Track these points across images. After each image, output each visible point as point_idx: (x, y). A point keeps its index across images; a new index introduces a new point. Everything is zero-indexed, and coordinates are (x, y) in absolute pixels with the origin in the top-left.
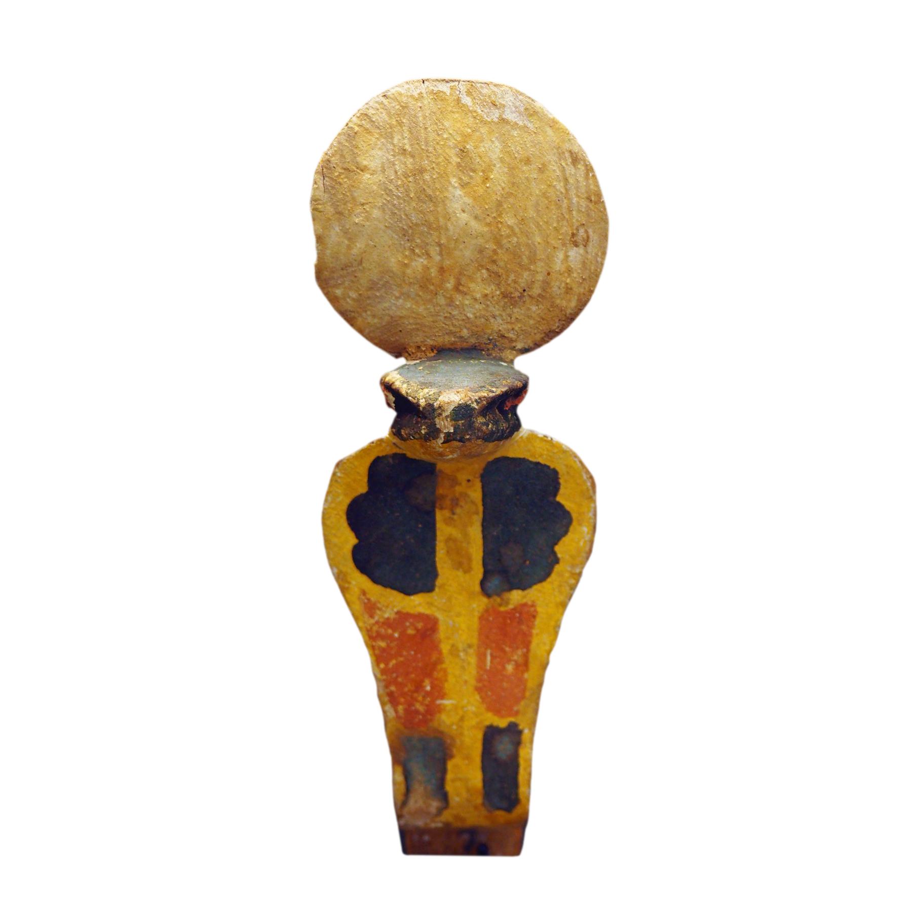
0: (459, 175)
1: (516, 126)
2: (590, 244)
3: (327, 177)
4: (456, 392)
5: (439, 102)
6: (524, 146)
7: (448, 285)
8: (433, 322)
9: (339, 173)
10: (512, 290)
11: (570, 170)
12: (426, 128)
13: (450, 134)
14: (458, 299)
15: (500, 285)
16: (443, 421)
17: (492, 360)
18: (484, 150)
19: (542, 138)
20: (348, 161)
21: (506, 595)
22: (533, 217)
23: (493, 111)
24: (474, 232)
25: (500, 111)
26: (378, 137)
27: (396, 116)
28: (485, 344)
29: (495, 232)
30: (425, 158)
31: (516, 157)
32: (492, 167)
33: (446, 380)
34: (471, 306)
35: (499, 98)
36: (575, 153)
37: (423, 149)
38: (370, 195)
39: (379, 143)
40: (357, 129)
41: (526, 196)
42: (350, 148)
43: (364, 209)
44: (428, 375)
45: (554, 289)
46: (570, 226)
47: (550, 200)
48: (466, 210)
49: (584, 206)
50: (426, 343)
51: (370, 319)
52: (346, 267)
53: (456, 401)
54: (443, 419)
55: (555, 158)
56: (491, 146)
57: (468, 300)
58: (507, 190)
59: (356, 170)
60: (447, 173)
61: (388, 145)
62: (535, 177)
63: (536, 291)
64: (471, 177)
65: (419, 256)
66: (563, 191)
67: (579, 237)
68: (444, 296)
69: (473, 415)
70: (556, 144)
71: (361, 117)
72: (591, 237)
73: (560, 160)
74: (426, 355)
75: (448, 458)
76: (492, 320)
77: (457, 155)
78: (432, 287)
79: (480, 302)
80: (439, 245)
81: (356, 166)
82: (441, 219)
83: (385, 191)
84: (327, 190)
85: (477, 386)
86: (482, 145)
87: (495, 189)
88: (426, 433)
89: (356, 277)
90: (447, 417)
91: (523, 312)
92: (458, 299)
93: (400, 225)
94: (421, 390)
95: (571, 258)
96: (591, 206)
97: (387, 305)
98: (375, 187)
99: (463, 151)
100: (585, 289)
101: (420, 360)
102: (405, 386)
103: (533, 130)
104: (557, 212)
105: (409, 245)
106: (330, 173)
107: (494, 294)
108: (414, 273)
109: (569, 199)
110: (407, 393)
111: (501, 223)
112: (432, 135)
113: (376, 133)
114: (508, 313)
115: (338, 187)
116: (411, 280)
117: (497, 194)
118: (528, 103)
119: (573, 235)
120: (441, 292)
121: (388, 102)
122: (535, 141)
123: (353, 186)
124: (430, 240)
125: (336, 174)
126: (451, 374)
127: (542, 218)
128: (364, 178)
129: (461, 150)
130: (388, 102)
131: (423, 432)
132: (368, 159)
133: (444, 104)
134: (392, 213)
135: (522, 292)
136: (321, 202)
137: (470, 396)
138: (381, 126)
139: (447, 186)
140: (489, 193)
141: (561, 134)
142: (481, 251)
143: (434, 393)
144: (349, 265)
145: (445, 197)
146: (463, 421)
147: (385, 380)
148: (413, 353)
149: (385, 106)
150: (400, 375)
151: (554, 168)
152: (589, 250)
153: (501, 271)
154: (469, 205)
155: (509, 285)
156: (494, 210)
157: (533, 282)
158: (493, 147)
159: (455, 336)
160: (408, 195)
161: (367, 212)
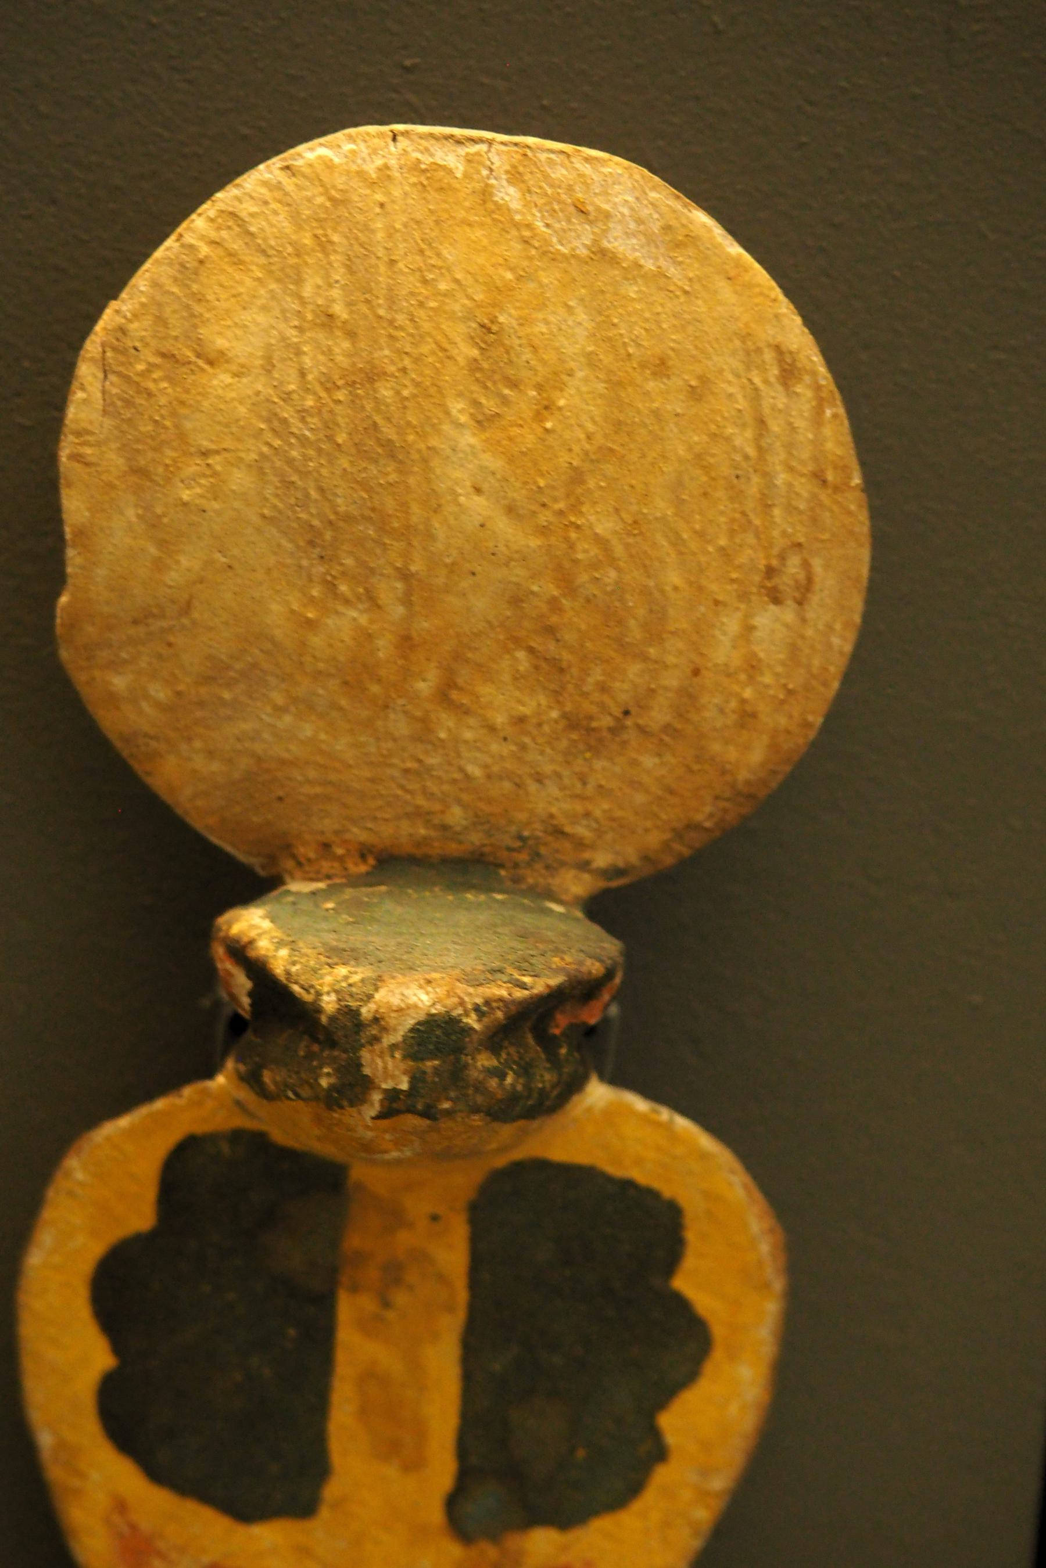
0: (472, 392)
1: (635, 273)
2: (815, 599)
3: (114, 372)
4: (422, 982)
5: (432, 192)
6: (654, 327)
7: (421, 686)
8: (372, 780)
9: (149, 364)
10: (594, 709)
11: (774, 398)
12: (393, 262)
13: (457, 281)
14: (445, 724)
15: (561, 694)
16: (381, 1056)
17: (524, 893)
18: (544, 330)
19: (704, 309)
20: (174, 334)
21: (514, 1541)
22: (663, 519)
23: (579, 227)
24: (502, 548)
25: (596, 230)
26: (260, 275)
27: (314, 224)
28: (510, 849)
29: (559, 553)
30: (383, 341)
31: (629, 355)
32: (565, 378)
33: (399, 944)
34: (478, 744)
35: (595, 194)
36: (791, 353)
37: (380, 317)
38: (226, 430)
39: (262, 292)
40: (204, 250)
41: (649, 459)
42: (184, 300)
43: (208, 465)
44: (349, 927)
45: (707, 714)
46: (765, 548)
47: (713, 474)
48: (485, 486)
49: (805, 494)
50: (347, 836)
51: (199, 762)
52: (146, 617)
53: (420, 1005)
54: (381, 1052)
55: (736, 364)
56: (565, 321)
57: (470, 727)
58: (599, 440)
59: (193, 359)
60: (441, 384)
61: (289, 299)
62: (679, 411)
63: (659, 715)
64: (505, 401)
65: (347, 602)
66: (751, 451)
67: (785, 579)
68: (405, 712)
69: (464, 1048)
70: (741, 325)
71: (220, 220)
72: (817, 579)
73: (748, 369)
74: (346, 869)
75: (387, 1157)
76: (533, 787)
77: (472, 338)
78: (375, 689)
79: (502, 734)
80: (405, 576)
81: (195, 351)
82: (415, 508)
83: (268, 421)
84: (111, 409)
85: (481, 967)
86: (540, 316)
87: (567, 435)
88: (332, 1088)
89: (170, 645)
90: (393, 1047)
91: (617, 769)
92: (445, 724)
93: (303, 516)
94: (326, 969)
95: (758, 634)
96: (824, 497)
97: (247, 726)
98: (242, 410)
99: (489, 331)
100: (790, 717)
101: (329, 882)
102: (284, 953)
103: (680, 283)
104: (730, 506)
105: (322, 569)
106: (123, 364)
107: (544, 718)
108: (331, 646)
109: (765, 475)
110: (288, 973)
111: (578, 527)
112: (409, 283)
113: (257, 265)
114: (577, 769)
115: (143, 402)
116: (321, 666)
117: (570, 450)
118: (674, 211)
119: (770, 572)
120: (401, 702)
121: (296, 185)
122: (686, 316)
123: (182, 403)
124: (382, 561)
125: (140, 367)
126: (412, 931)
127: (688, 522)
128: (215, 382)
129: (483, 326)
130: (296, 185)
131: (324, 1082)
132: (229, 334)
133: (445, 202)
134: (283, 481)
135: (620, 716)
136: (90, 438)
137: (462, 995)
138: (272, 247)
139: (438, 418)
140: (551, 447)
141: (757, 301)
142: (516, 601)
143: (363, 981)
144: (155, 611)
145: (429, 448)
146: (437, 1062)
147: (230, 927)
148: (309, 860)
149: (286, 194)
150: (272, 922)
151: (731, 390)
152: (810, 615)
153: (566, 656)
154: (493, 473)
155: (585, 695)
156: (560, 493)
157: (653, 691)
158: (570, 323)
159: (428, 824)
160: (330, 438)
161: (215, 474)
